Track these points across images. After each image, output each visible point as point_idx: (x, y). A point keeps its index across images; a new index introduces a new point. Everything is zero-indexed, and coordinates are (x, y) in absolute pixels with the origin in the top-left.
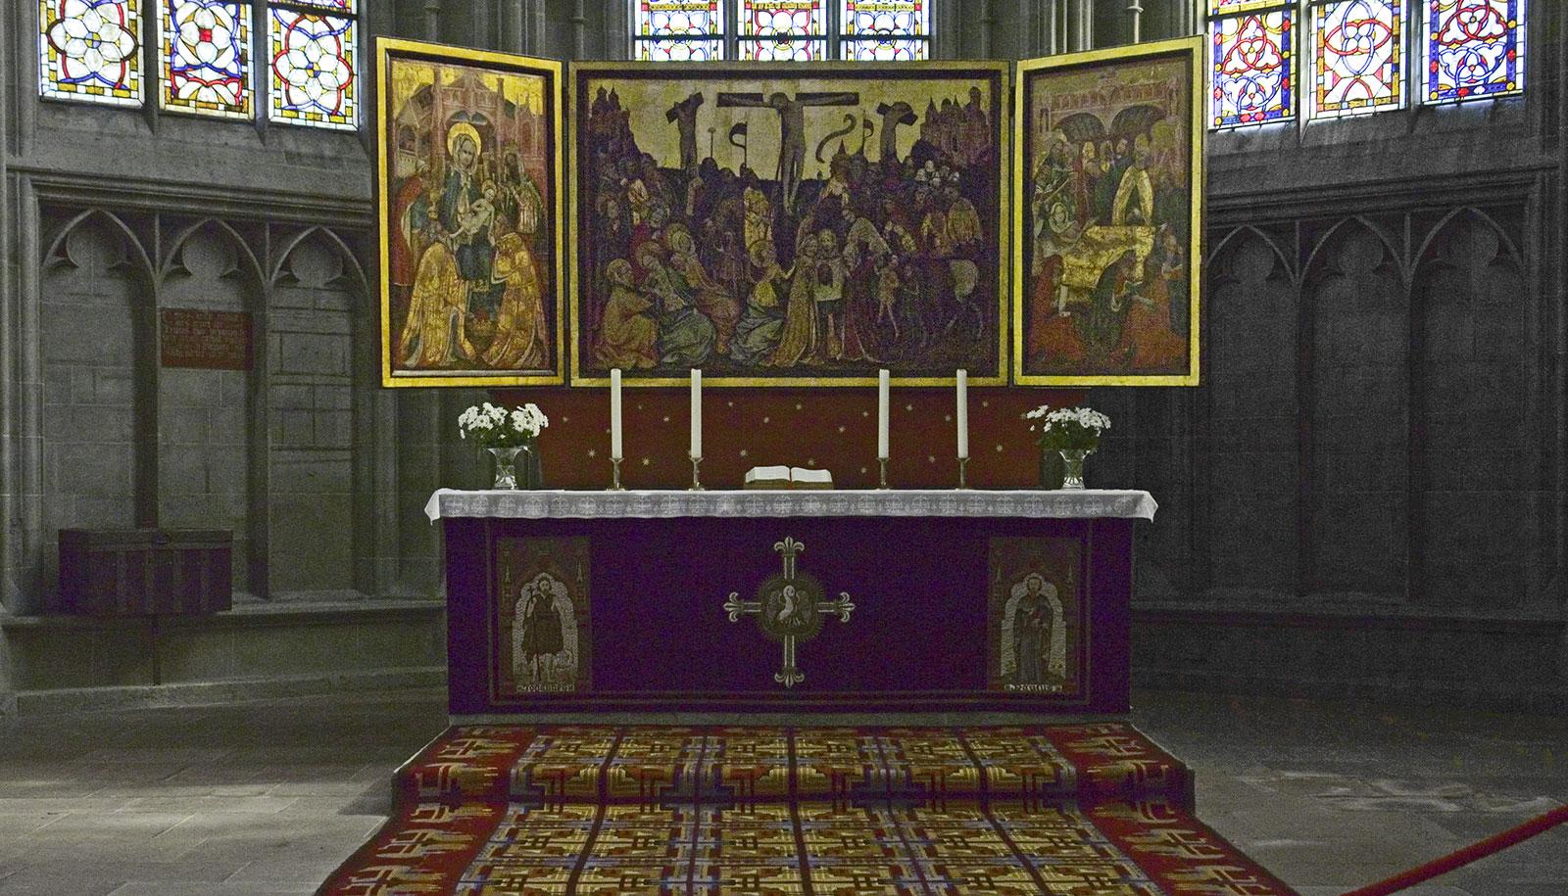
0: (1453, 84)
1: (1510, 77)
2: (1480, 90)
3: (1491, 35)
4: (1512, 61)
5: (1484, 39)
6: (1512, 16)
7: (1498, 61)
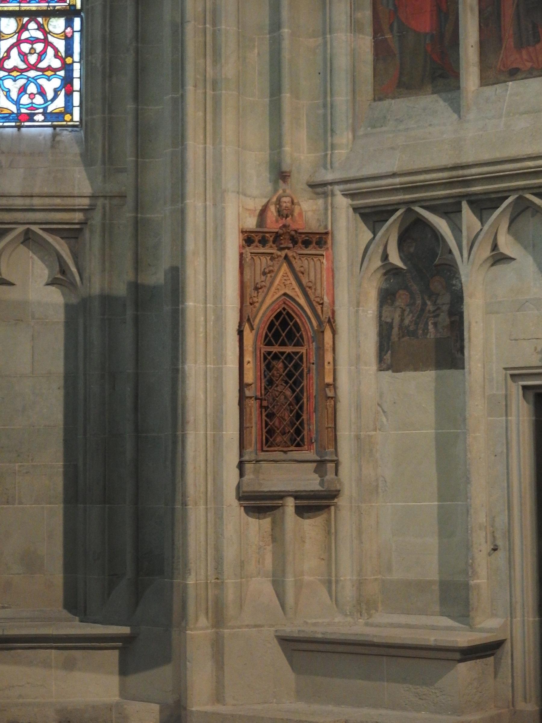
0: (14, 109)
1: (68, 108)
2: (40, 117)
3: (49, 68)
4: (69, 95)
5: (43, 70)
6: (69, 51)
7: (56, 92)
